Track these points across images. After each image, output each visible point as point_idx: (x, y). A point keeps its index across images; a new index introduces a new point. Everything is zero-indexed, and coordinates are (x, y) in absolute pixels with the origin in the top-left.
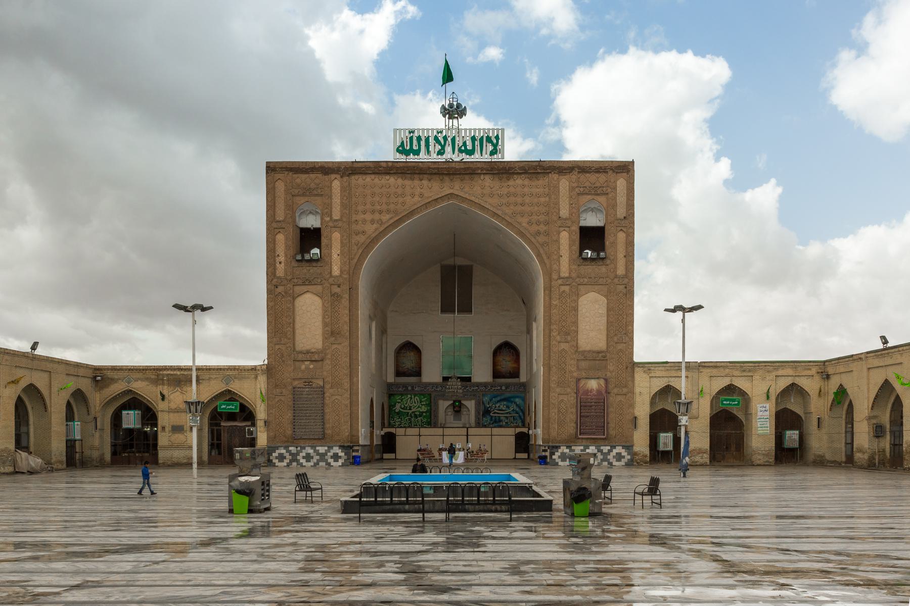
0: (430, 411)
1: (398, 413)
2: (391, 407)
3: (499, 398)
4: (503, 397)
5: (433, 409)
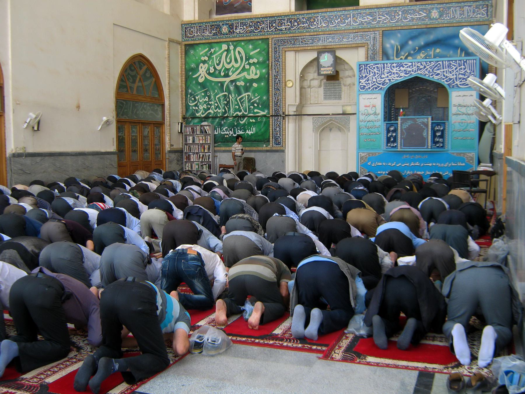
0: (265, 78)
1: (203, 85)
2: (189, 73)
3: (422, 41)
4: (432, 37)
5: (272, 73)
